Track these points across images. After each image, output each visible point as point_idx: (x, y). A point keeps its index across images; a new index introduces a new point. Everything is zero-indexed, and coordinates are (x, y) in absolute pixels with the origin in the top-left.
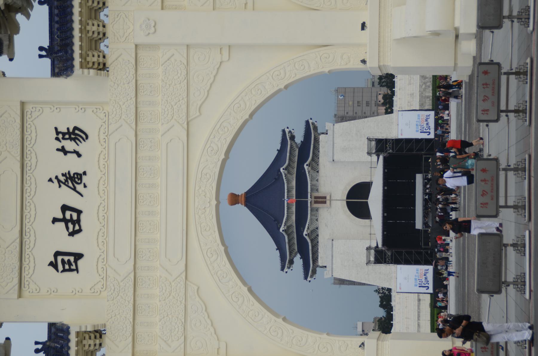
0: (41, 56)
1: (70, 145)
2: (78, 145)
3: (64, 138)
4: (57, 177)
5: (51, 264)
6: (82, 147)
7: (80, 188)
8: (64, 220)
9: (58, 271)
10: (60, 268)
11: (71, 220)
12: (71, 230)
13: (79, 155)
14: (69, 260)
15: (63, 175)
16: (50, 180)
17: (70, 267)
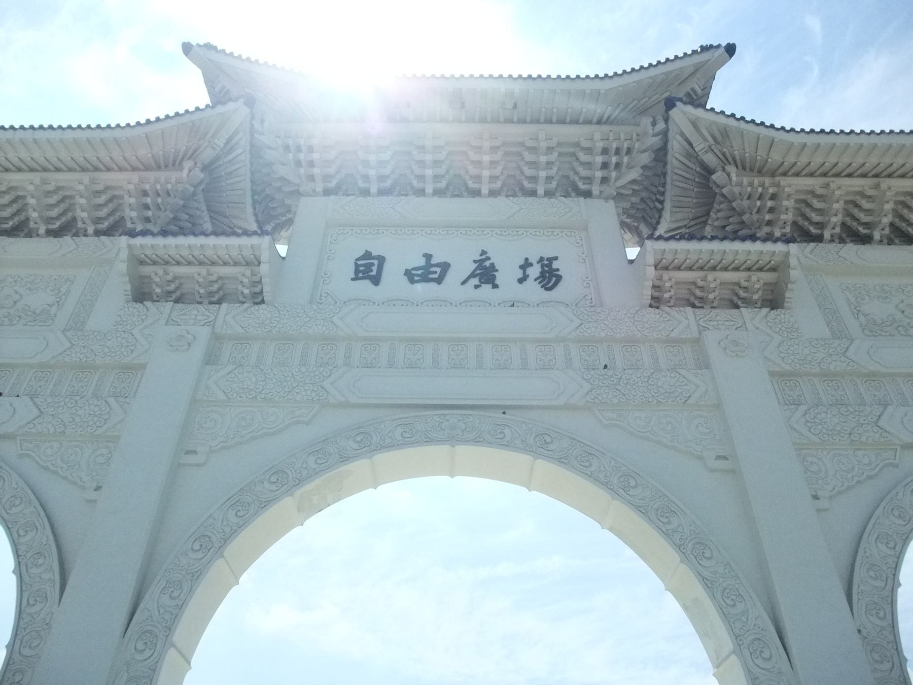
1: (534, 271)
2: (536, 280)
3: (543, 266)
4: (488, 258)
9: (358, 259)
10: (360, 262)
12: (413, 272)
13: (521, 281)
14: (372, 271)
15: (492, 265)
16: (484, 252)
17: (360, 271)
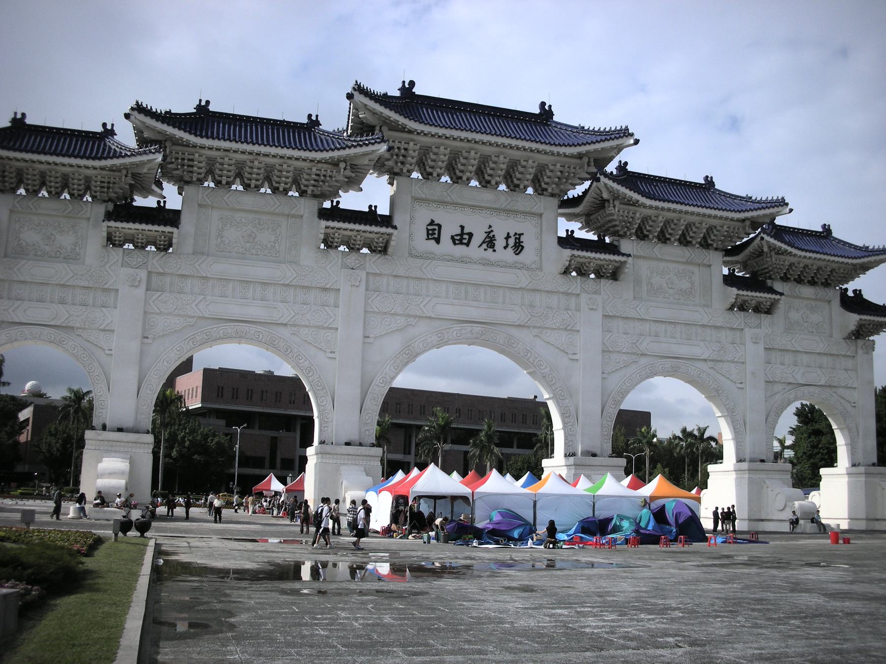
0: (567, 231)
1: (512, 242)
5: (432, 221)
6: (509, 249)
7: (485, 246)
8: (462, 234)
10: (430, 227)
11: (463, 238)
13: (505, 248)
16: (490, 227)
